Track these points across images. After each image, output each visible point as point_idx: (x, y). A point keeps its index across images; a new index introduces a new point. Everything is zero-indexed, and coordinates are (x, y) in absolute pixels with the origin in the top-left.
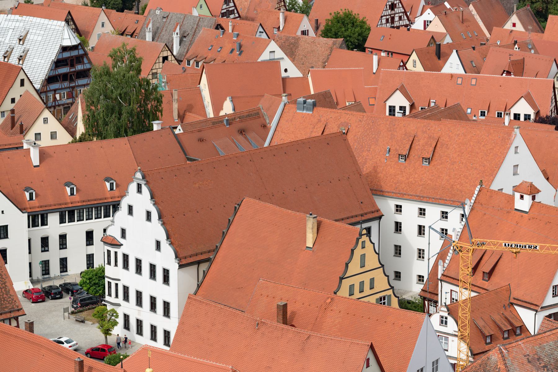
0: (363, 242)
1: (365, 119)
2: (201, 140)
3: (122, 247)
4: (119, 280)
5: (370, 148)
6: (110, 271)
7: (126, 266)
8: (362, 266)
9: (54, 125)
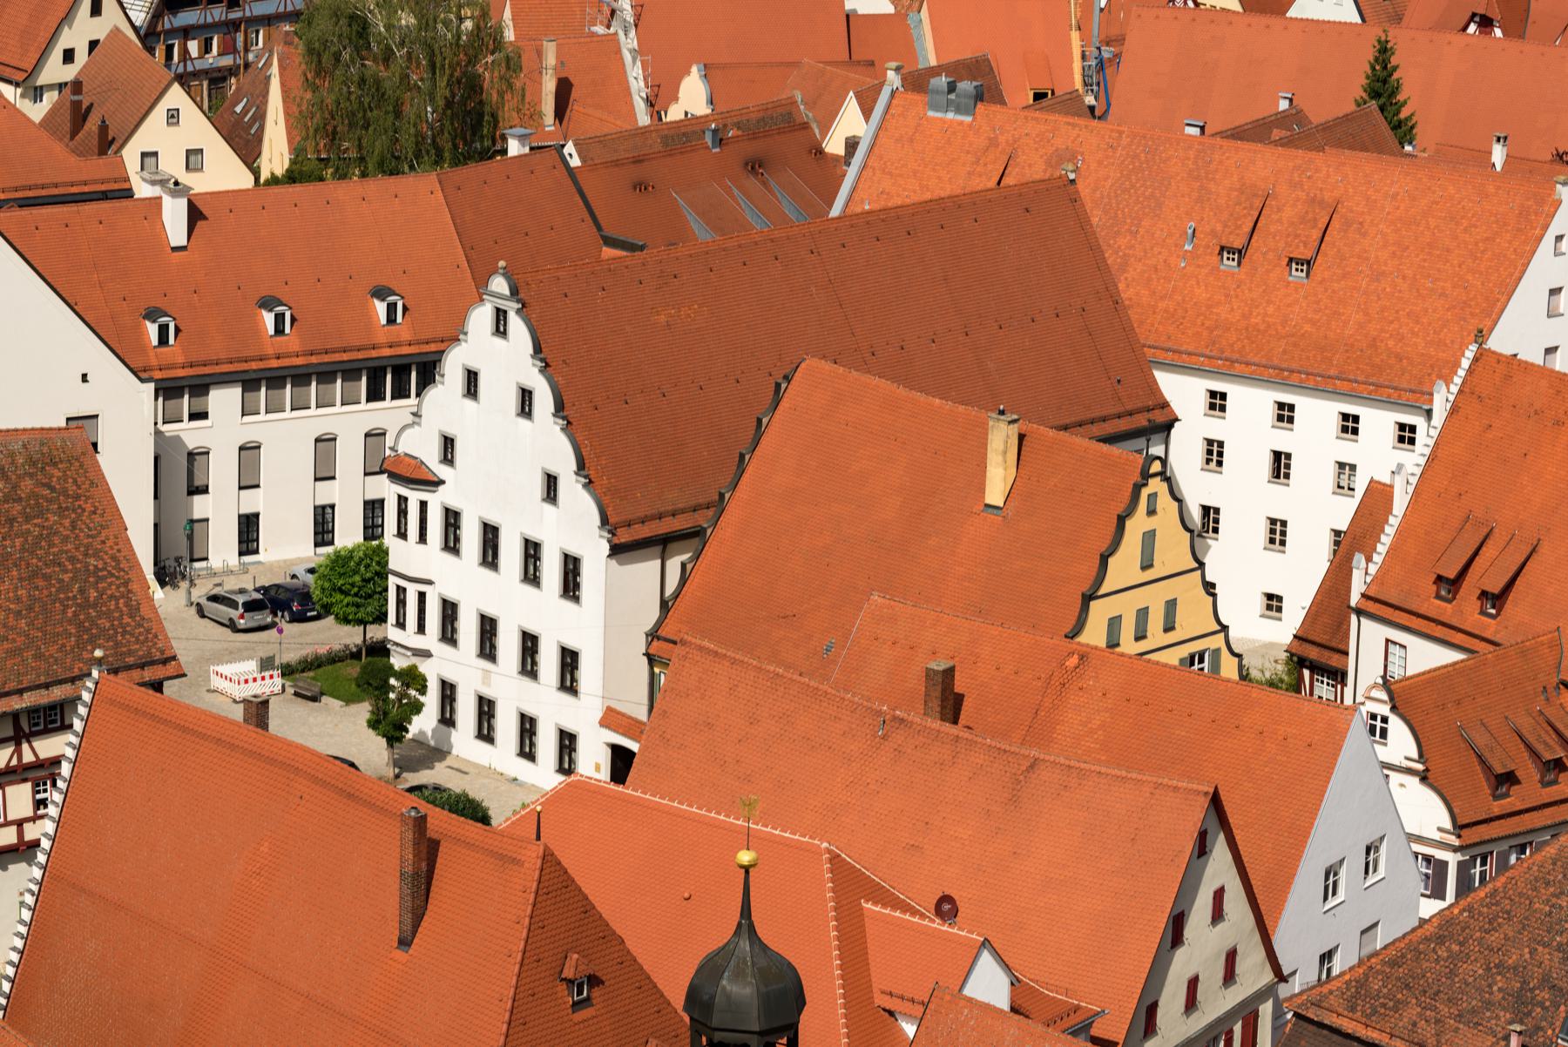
0: (1153, 497)
1: (1125, 141)
2: (640, 186)
3: (441, 488)
4: (430, 582)
5: (1139, 226)
6: (404, 556)
7: (452, 545)
8: (1147, 565)
9: (196, 128)
